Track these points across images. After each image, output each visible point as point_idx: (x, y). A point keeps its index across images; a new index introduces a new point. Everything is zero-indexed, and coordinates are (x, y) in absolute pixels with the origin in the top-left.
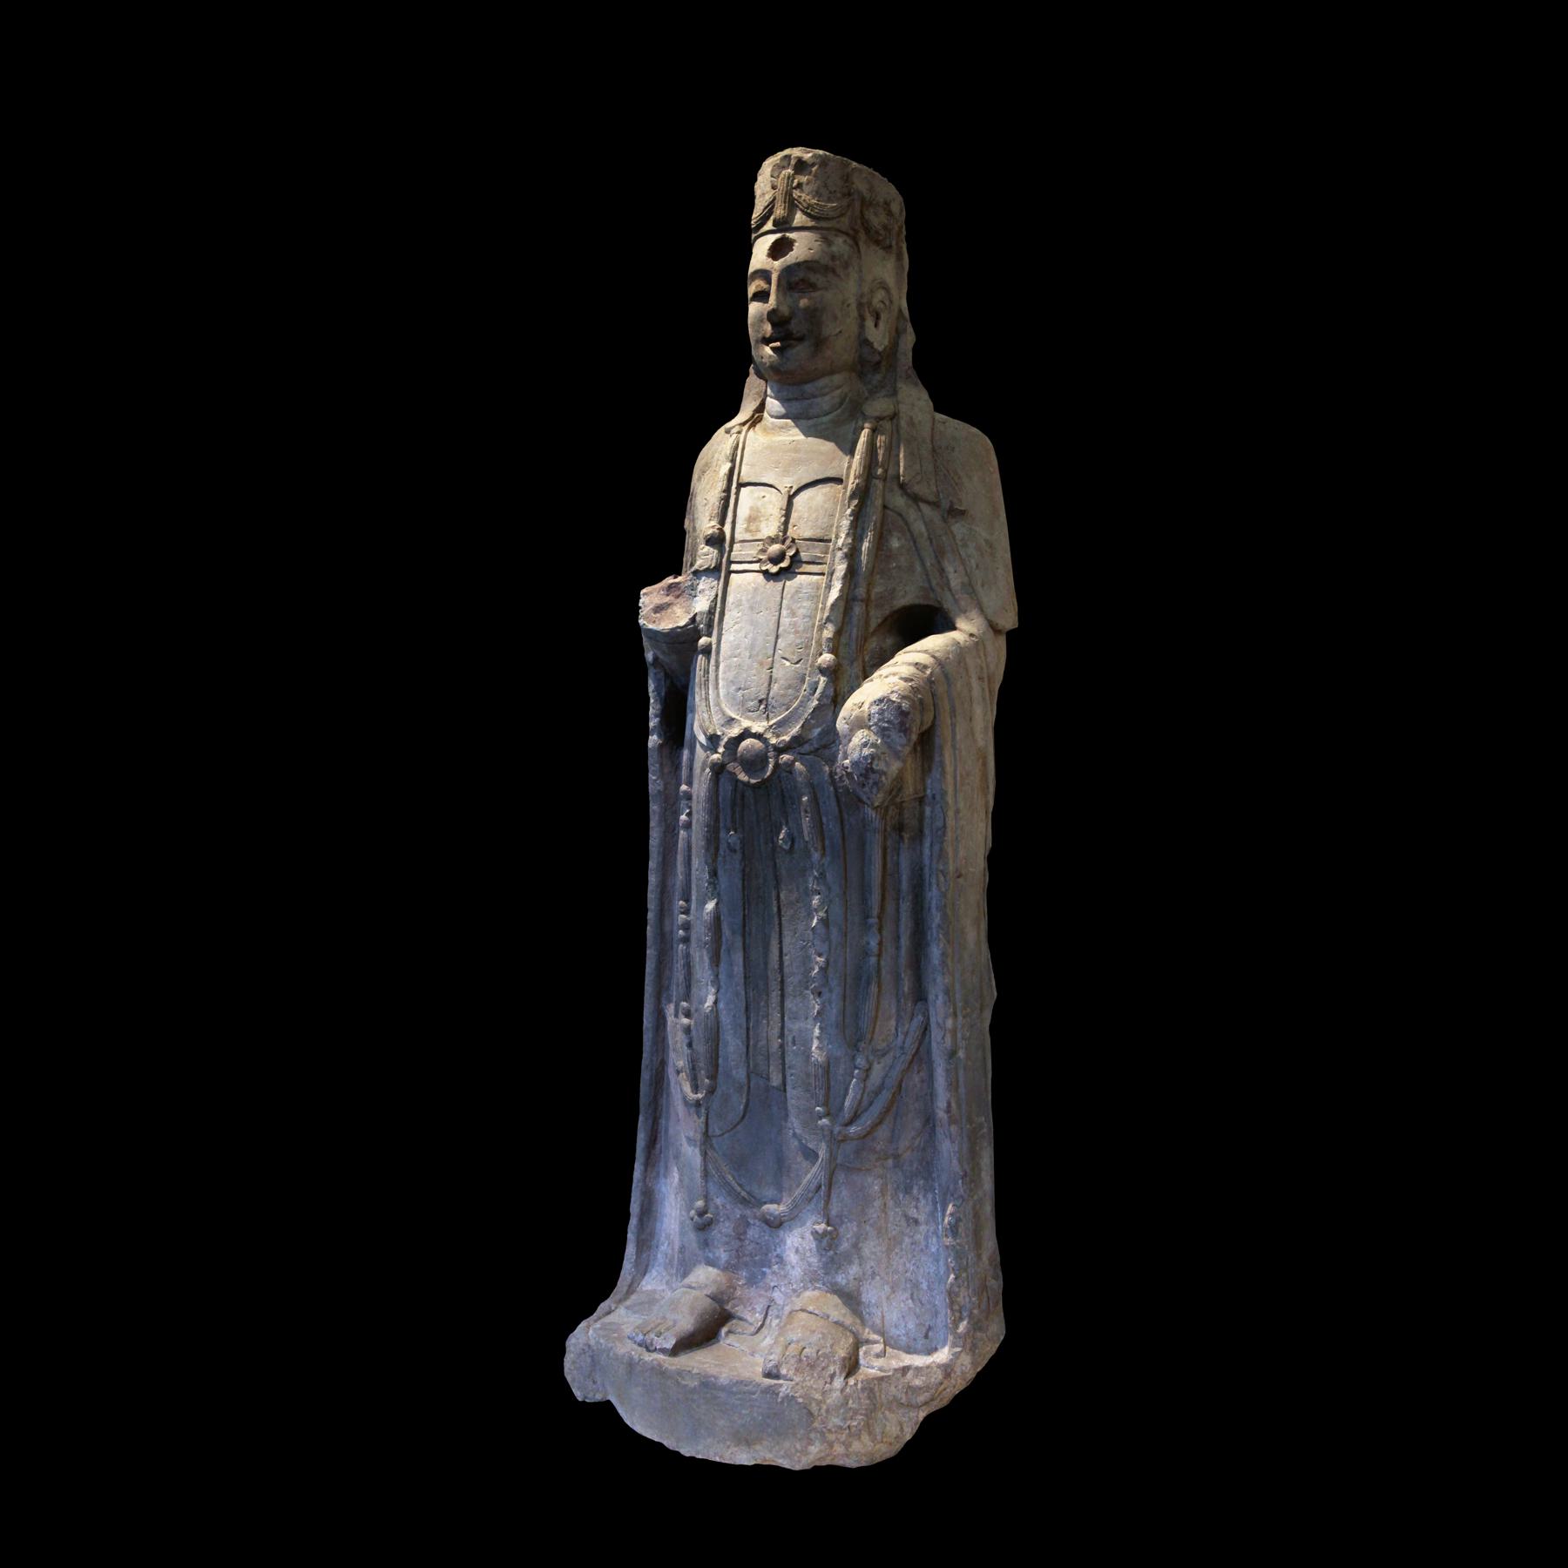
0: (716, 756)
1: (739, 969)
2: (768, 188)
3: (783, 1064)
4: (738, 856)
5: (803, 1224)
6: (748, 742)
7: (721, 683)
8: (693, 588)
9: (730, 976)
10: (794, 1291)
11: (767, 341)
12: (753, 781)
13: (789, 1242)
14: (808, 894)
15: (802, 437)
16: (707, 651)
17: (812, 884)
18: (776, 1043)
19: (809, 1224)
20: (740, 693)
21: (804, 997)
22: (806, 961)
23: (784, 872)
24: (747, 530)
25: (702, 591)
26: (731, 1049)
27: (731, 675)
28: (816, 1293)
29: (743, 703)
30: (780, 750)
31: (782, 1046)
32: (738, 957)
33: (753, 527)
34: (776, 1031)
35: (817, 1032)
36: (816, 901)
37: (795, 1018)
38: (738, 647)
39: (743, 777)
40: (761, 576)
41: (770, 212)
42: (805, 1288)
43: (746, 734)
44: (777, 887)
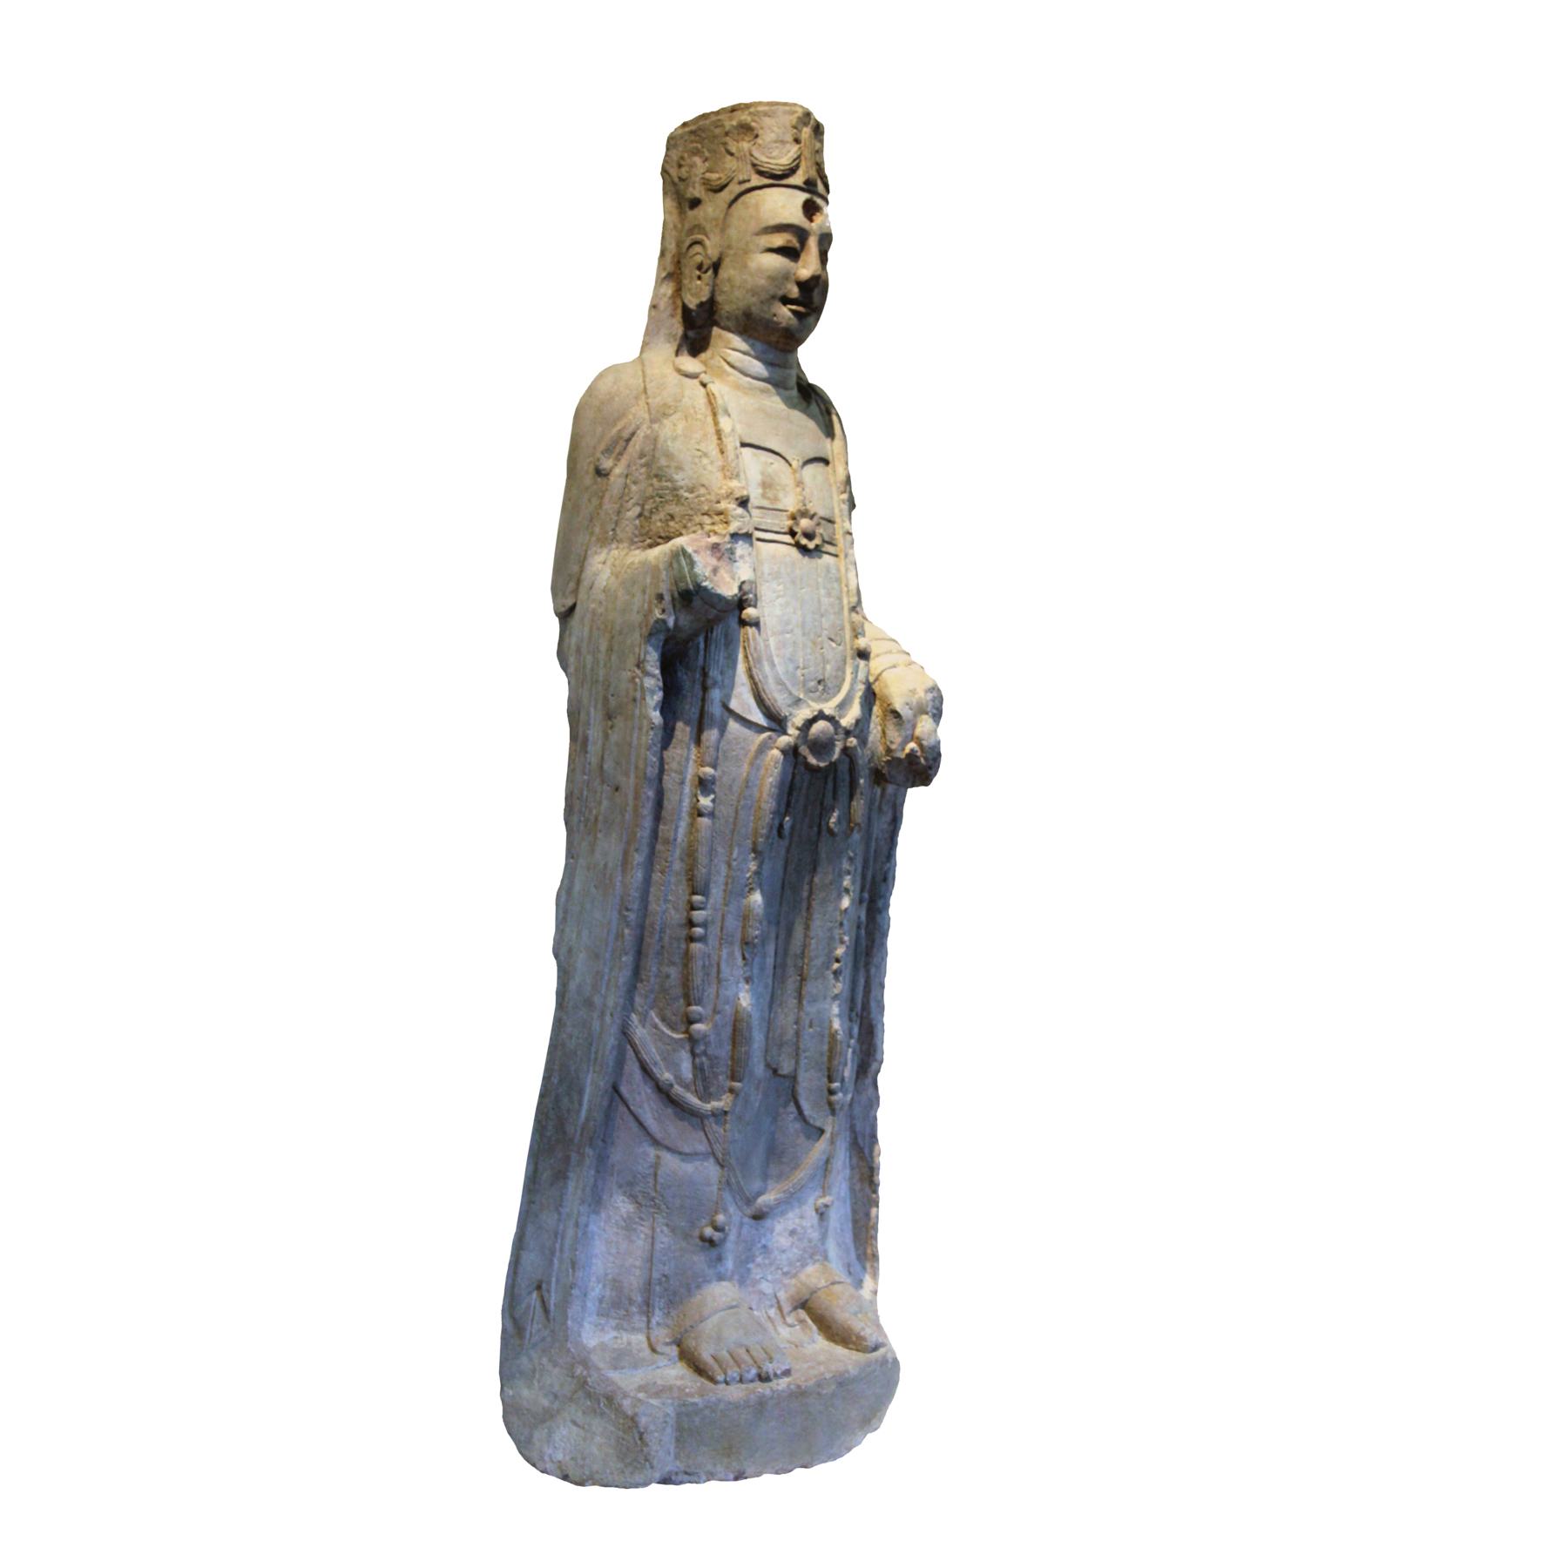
0: (784, 740)
1: (770, 961)
2: (789, 138)
3: (798, 1048)
4: (785, 843)
5: (801, 1202)
6: (821, 725)
7: (776, 661)
8: (732, 551)
9: (762, 969)
10: (785, 1274)
11: (785, 300)
12: (822, 765)
13: (778, 1227)
14: (840, 876)
15: (782, 406)
16: (756, 624)
17: (846, 865)
18: (791, 1032)
19: (811, 1201)
20: (799, 672)
21: (824, 978)
22: (831, 942)
23: (823, 855)
24: (764, 496)
25: (742, 557)
26: (756, 1046)
27: (788, 651)
28: (817, 1265)
29: (804, 683)
30: (848, 733)
31: (798, 1034)
32: (771, 948)
33: (770, 494)
34: (791, 1019)
35: (836, 1010)
36: (847, 882)
37: (814, 1000)
38: (788, 623)
39: (812, 760)
40: (794, 552)
41: (797, 167)
42: (804, 1266)
43: (821, 716)
44: (814, 870)
